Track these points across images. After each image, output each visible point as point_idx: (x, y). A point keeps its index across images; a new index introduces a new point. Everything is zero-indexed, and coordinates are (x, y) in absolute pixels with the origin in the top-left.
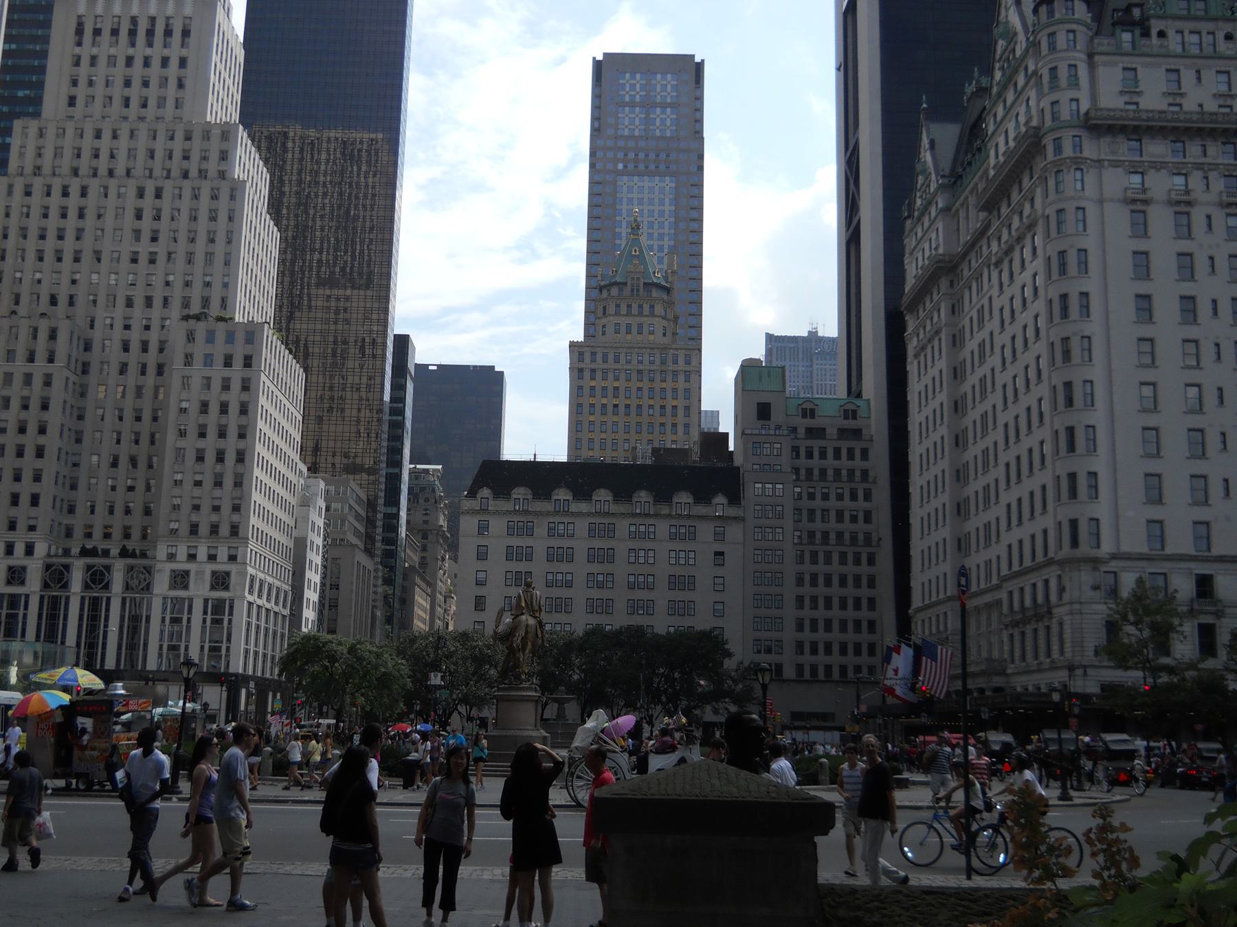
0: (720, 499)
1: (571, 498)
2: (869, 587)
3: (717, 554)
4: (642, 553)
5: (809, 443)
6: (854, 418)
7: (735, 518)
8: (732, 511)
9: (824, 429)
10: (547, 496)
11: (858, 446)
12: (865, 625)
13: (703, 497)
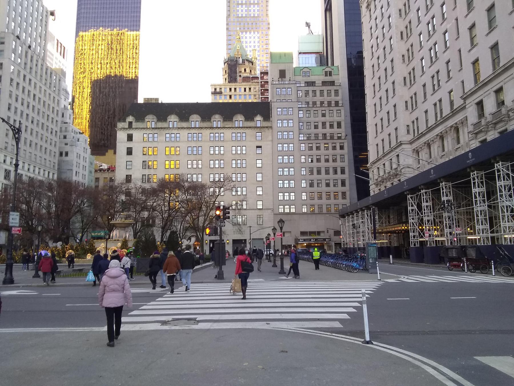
0: (259, 118)
1: (177, 120)
2: (342, 173)
3: (258, 147)
4: (217, 148)
5: (307, 88)
6: (330, 74)
7: (267, 127)
8: (266, 124)
9: (315, 82)
10: (165, 120)
11: (332, 88)
12: (340, 194)
13: (249, 117)
